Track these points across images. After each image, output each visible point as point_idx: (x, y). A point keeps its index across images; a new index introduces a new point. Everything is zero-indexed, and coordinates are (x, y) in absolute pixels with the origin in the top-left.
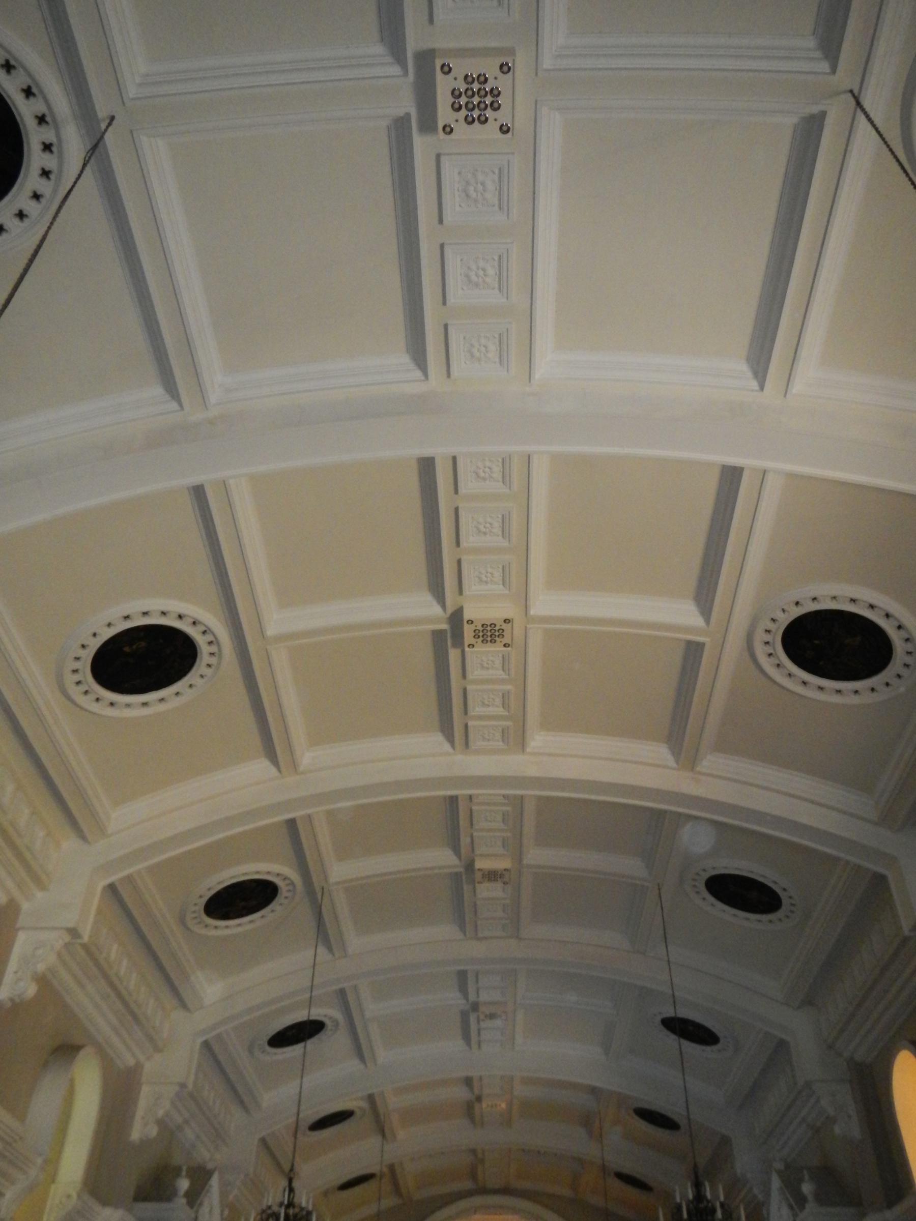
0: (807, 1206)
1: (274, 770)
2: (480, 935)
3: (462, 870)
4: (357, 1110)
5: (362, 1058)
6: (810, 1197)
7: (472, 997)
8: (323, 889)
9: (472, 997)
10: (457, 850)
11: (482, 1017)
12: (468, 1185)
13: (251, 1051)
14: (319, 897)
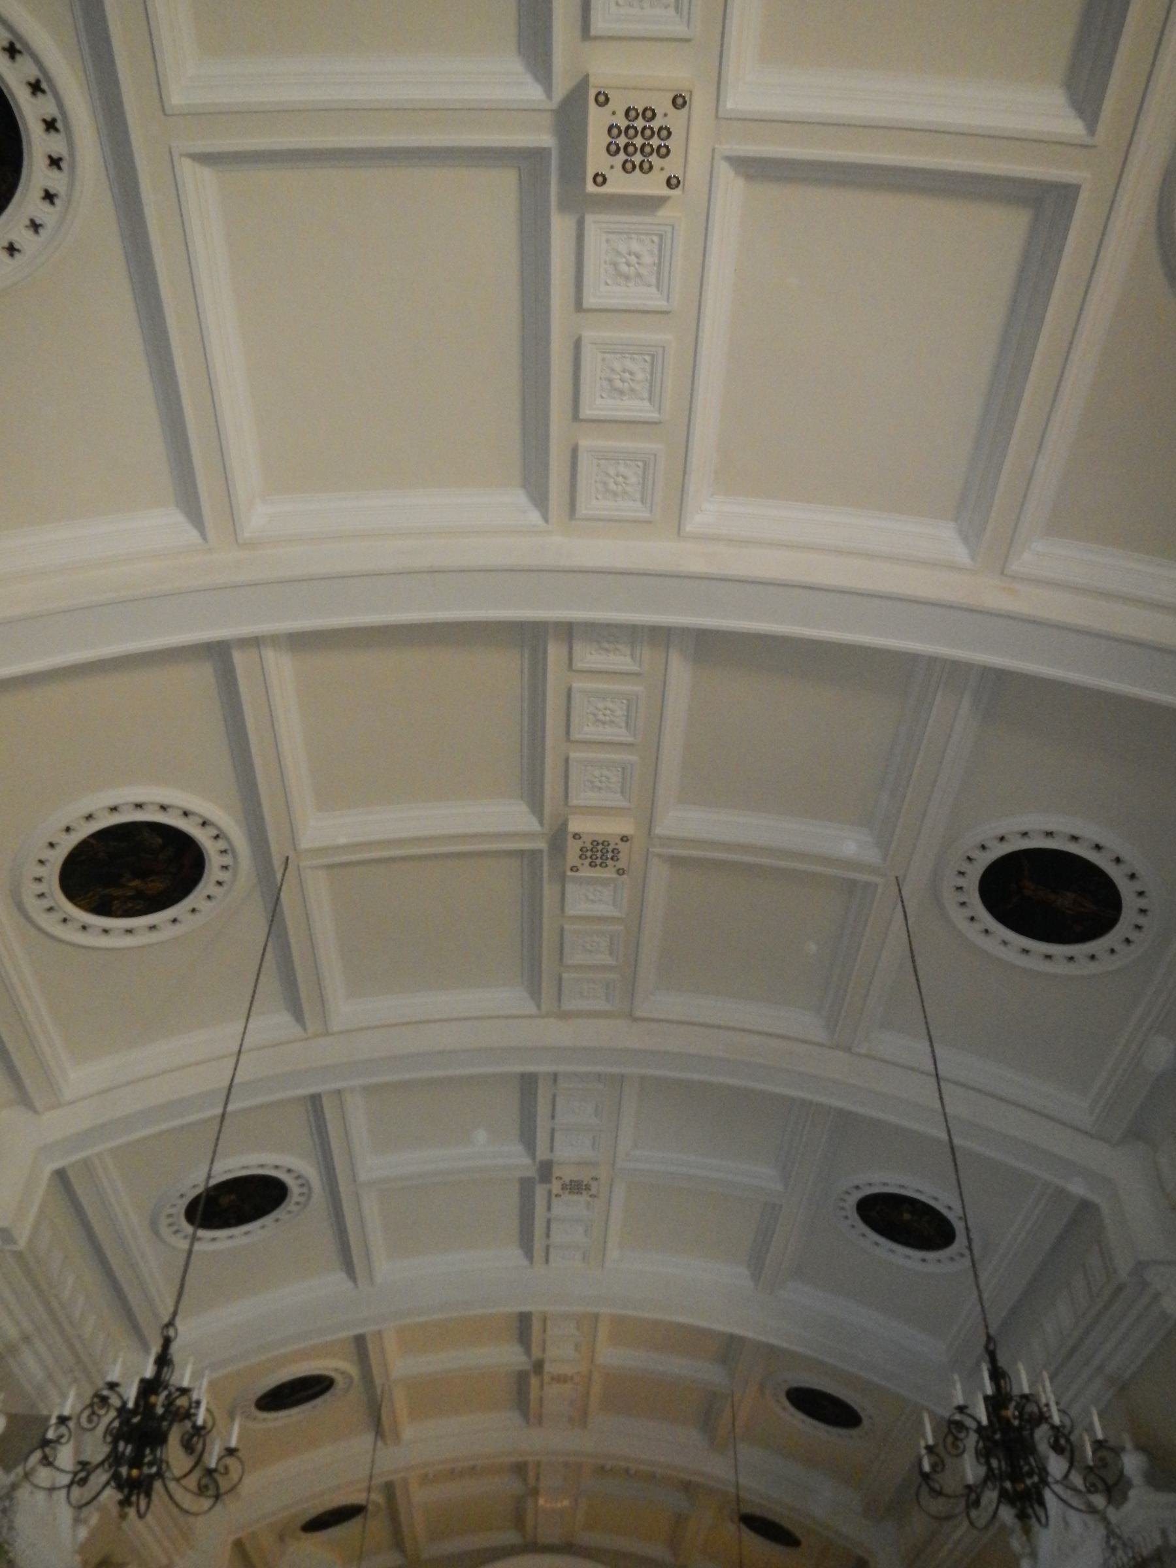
0: (1132, 1493)
1: (193, 535)
2: (569, 1005)
3: (542, 845)
4: (338, 1378)
5: (349, 1267)
6: (1137, 1479)
7: (542, 1153)
8: (287, 859)
9: (542, 1153)
10: (536, 805)
11: (556, 1187)
12: (511, 1537)
13: (154, 1225)
14: (279, 876)
